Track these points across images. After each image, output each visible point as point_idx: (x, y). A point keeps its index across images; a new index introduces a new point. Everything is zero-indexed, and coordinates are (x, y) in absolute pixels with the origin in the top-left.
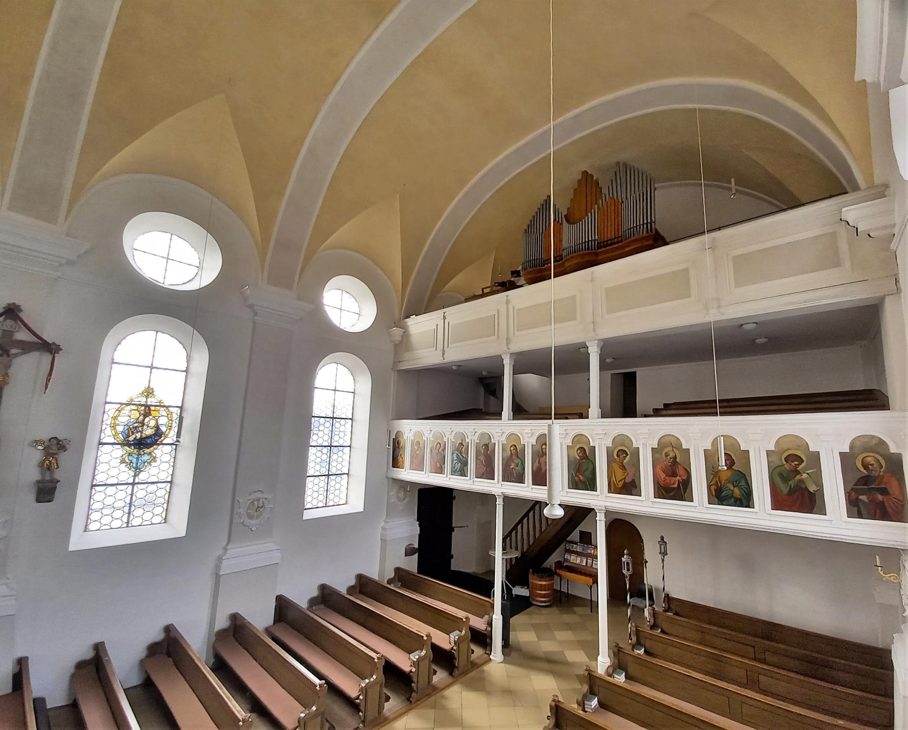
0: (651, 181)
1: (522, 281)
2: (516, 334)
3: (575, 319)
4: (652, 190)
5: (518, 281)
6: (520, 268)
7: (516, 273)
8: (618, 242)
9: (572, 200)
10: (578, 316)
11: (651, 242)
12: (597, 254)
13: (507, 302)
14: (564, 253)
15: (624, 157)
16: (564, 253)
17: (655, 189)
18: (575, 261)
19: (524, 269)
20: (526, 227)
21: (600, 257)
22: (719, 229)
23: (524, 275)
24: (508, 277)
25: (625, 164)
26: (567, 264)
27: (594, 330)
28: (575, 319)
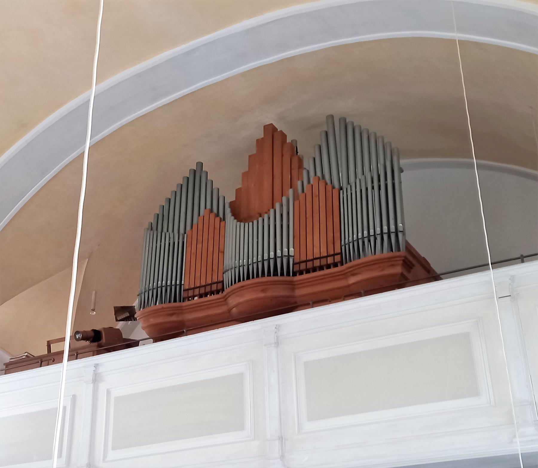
0: (394, 154)
1: (138, 331)
2: (112, 454)
3: (242, 428)
4: (394, 172)
5: (132, 330)
6: (136, 304)
7: (126, 313)
8: (335, 265)
9: (245, 175)
10: (248, 423)
11: (398, 270)
12: (292, 286)
13: (96, 379)
14: (227, 277)
15: (342, 107)
16: (227, 277)
17: (401, 171)
18: (248, 296)
19: (143, 305)
20: (151, 219)
21: (299, 292)
22: (522, 259)
23: (146, 317)
24: (104, 320)
25: (344, 121)
26: (233, 301)
27: (282, 457)
28: (242, 428)
